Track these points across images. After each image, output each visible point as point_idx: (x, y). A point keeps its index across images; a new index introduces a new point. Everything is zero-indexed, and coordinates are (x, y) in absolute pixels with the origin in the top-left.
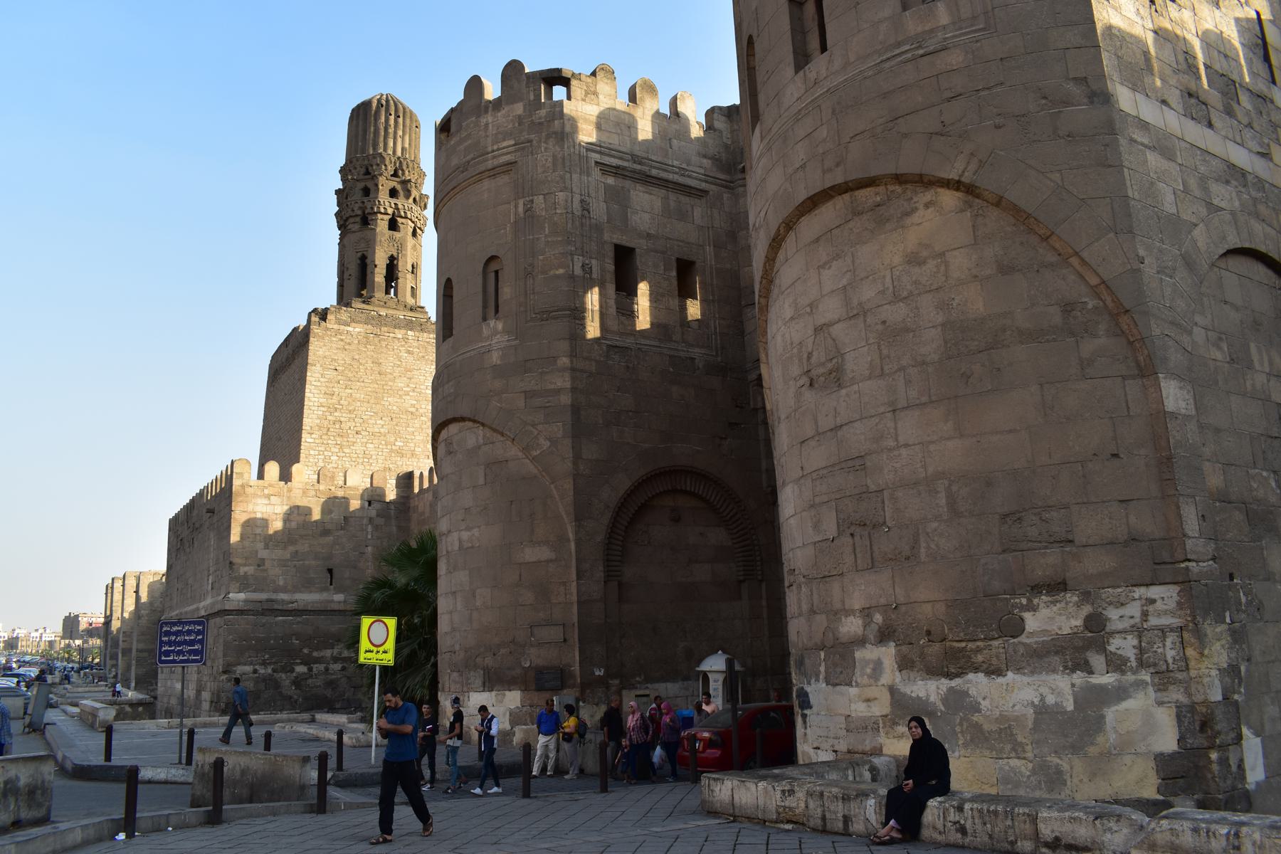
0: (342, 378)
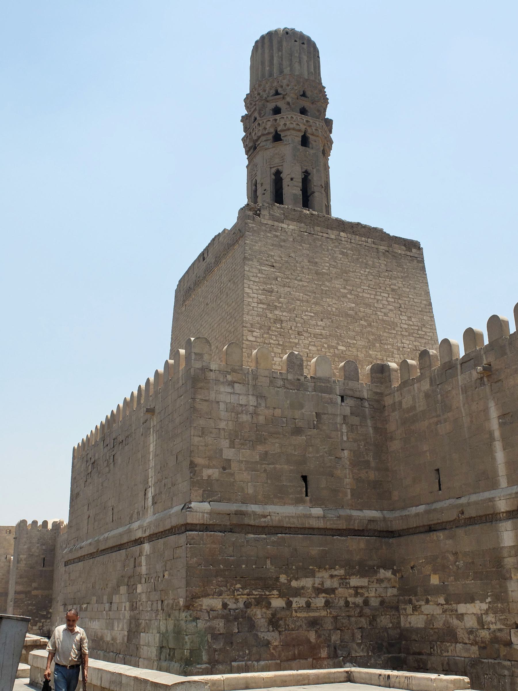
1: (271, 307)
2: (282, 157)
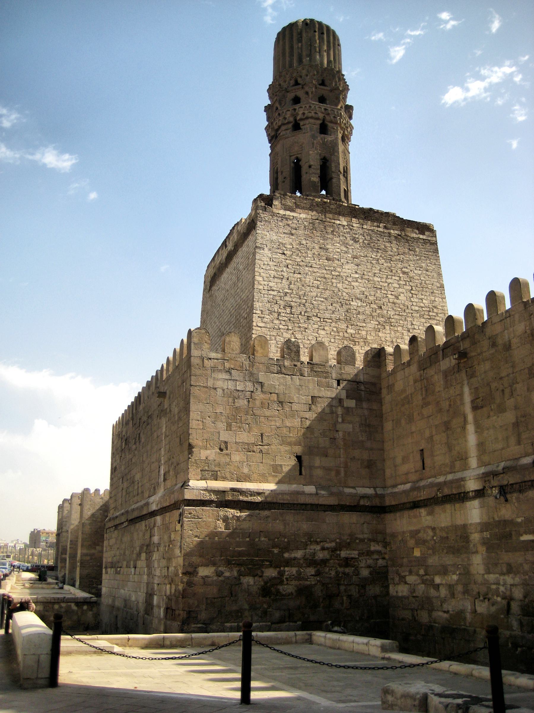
0: (290, 262)
1: (282, 294)
2: (301, 146)
